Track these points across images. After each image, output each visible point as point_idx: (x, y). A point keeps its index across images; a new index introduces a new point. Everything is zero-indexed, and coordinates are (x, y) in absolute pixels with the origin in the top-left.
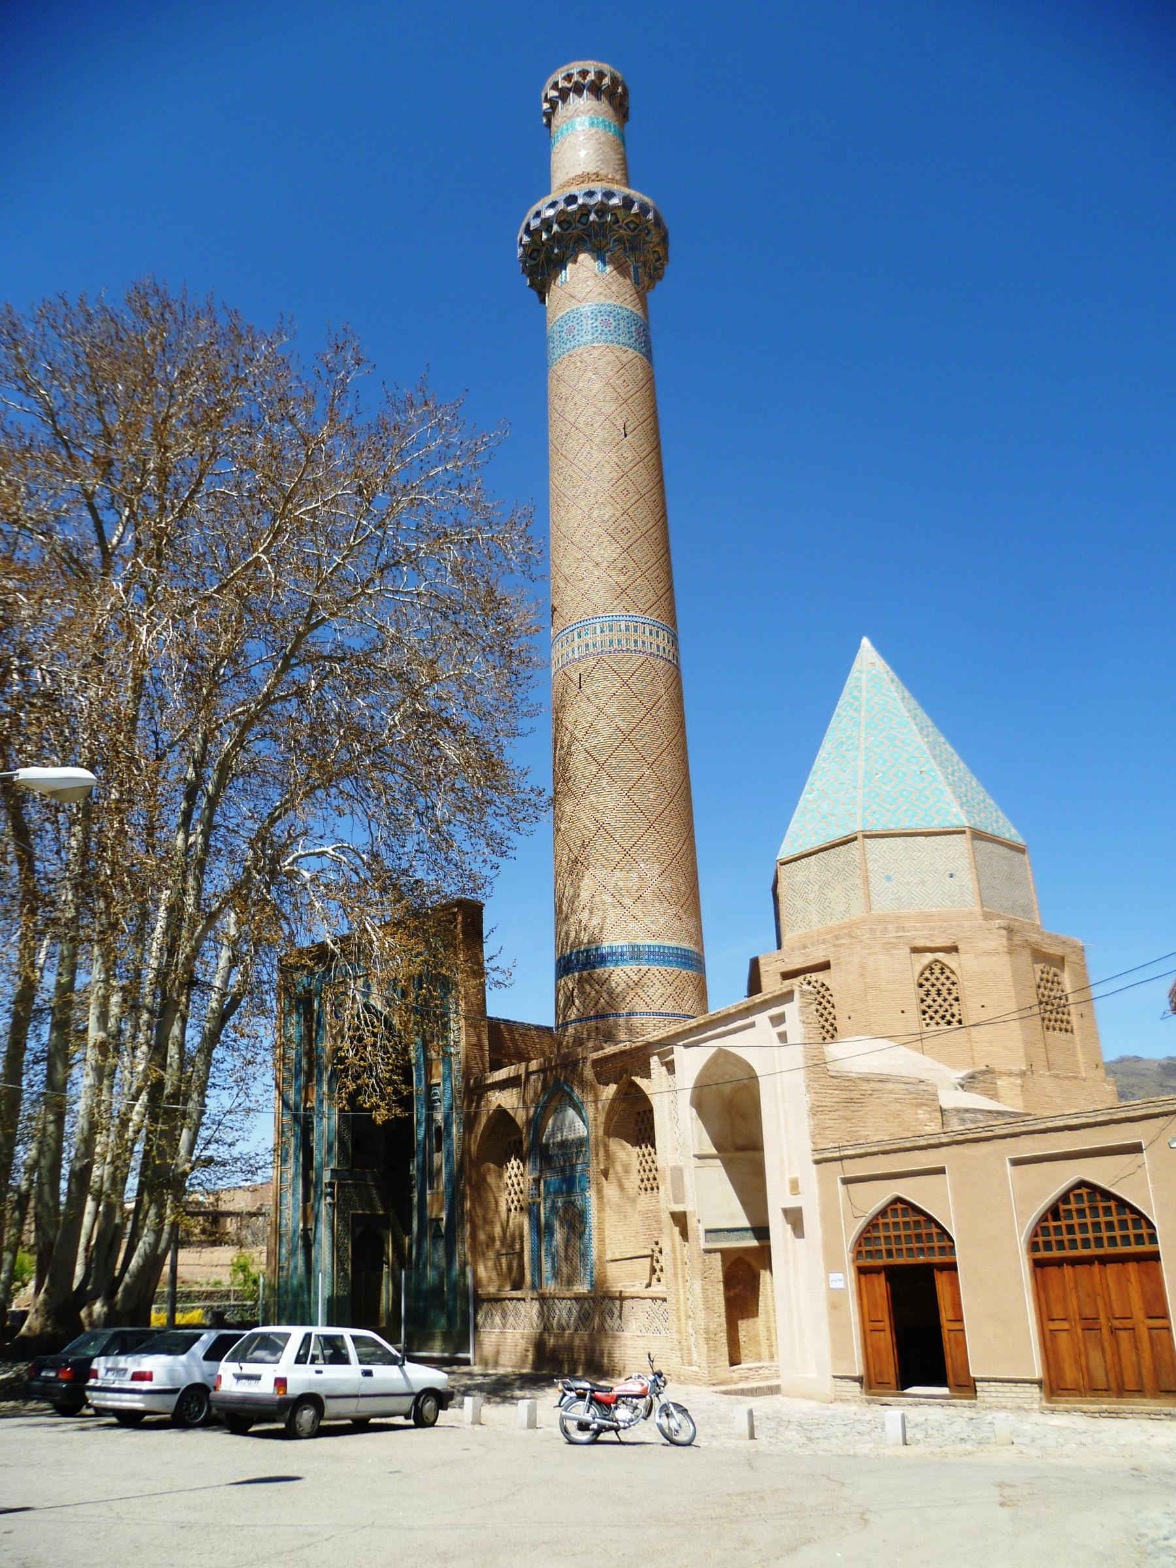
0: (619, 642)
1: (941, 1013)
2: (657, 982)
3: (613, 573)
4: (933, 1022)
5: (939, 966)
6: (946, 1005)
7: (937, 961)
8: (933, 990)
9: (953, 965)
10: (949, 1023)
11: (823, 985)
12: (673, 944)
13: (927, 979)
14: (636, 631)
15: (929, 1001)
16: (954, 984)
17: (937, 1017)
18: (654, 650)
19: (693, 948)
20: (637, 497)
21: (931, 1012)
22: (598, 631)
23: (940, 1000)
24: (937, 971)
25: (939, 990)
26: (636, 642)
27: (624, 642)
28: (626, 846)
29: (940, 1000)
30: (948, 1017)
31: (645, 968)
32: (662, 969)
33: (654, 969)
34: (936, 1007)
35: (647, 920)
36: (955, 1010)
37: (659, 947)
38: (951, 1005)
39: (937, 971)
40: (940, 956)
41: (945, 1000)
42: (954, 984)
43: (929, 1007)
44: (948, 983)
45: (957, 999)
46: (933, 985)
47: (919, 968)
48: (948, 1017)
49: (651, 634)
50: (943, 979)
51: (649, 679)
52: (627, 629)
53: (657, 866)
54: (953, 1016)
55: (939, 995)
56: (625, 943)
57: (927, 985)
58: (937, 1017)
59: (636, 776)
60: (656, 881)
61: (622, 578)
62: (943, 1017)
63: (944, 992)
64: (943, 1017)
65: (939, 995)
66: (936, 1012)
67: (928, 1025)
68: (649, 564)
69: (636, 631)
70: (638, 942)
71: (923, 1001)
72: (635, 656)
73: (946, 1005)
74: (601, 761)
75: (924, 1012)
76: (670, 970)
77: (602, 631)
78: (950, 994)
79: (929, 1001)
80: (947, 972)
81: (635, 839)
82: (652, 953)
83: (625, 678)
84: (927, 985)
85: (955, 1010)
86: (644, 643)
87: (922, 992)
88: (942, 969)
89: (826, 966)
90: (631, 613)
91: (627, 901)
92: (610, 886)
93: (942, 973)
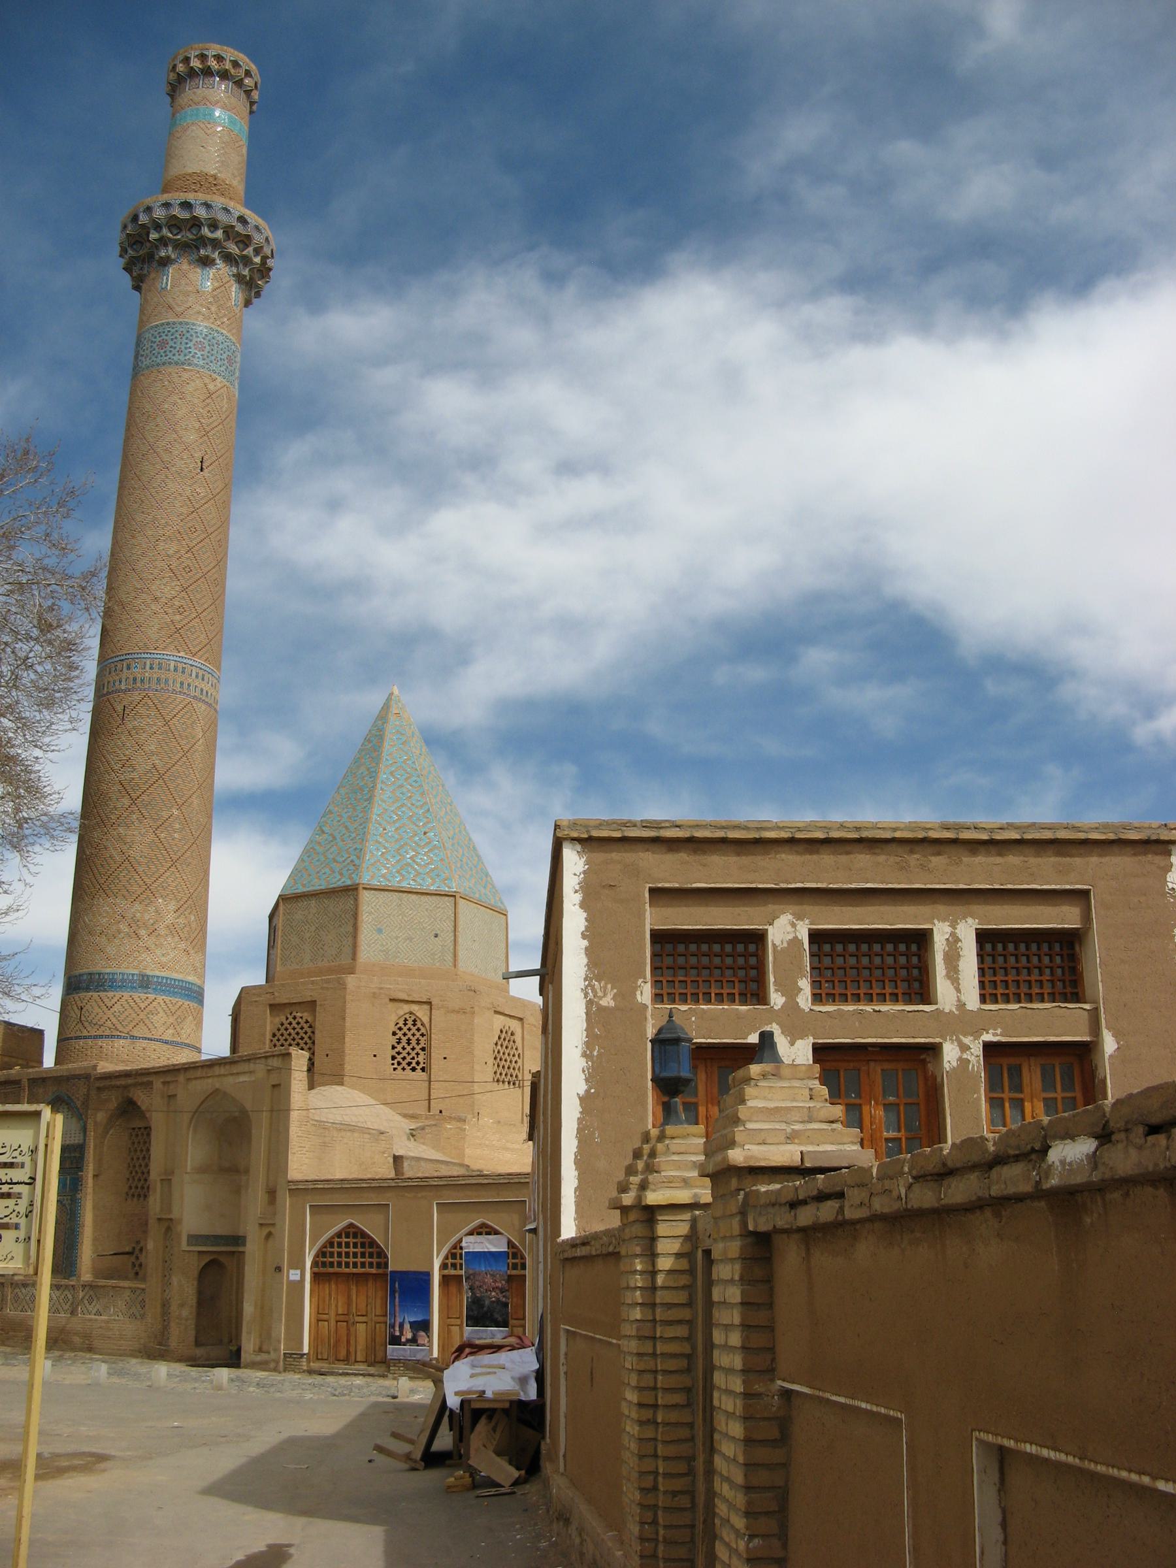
1: (408, 1060)
3: (170, 611)
4: (400, 1068)
6: (413, 1054)
7: (411, 1013)
8: (404, 1039)
9: (426, 1020)
10: (414, 1069)
11: (307, 1022)
13: (400, 1029)
15: (399, 1048)
16: (423, 1035)
17: (404, 1064)
19: (198, 982)
20: (202, 537)
21: (399, 1058)
23: (408, 1048)
24: (410, 1022)
25: (409, 1040)
28: (149, 881)
29: (408, 1048)
30: (414, 1065)
31: (152, 996)
32: (168, 999)
33: (160, 998)
34: (404, 1054)
35: (158, 952)
36: (421, 1059)
38: (418, 1054)
39: (410, 1022)
40: (415, 1008)
41: (413, 1049)
42: (423, 1035)
43: (399, 1053)
44: (418, 1034)
45: (423, 1049)
46: (405, 1035)
47: (394, 1018)
48: (414, 1065)
50: (414, 1029)
53: (173, 902)
54: (418, 1063)
55: (409, 1044)
56: (136, 972)
57: (400, 1034)
58: (404, 1064)
61: (178, 617)
62: (409, 1064)
63: (414, 1042)
64: (409, 1064)
65: (409, 1044)
66: (404, 1058)
67: (395, 1069)
68: (206, 606)
70: (149, 972)
71: (393, 1047)
73: (413, 1054)
75: (393, 1058)
76: (174, 1000)
78: (418, 1044)
79: (399, 1048)
80: (419, 1025)
81: (157, 875)
82: (160, 983)
84: (400, 1034)
85: (421, 1059)
87: (393, 1040)
88: (415, 1021)
89: (311, 1005)
91: (143, 932)
92: (129, 915)
93: (414, 1025)
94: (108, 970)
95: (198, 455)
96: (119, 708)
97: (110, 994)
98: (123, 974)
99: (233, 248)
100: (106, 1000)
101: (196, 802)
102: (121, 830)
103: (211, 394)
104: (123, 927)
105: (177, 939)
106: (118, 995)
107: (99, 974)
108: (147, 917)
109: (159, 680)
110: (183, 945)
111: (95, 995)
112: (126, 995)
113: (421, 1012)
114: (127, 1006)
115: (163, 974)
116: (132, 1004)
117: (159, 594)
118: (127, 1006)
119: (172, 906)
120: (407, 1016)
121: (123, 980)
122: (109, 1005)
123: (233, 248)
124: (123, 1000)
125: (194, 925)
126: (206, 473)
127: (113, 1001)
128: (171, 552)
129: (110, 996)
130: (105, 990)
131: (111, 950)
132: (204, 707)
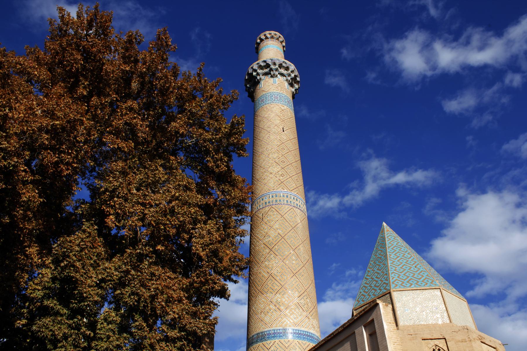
0: (280, 200)
2: (298, 348)
5: (438, 348)
12: (306, 330)
14: (287, 197)
18: (295, 205)
22: (271, 197)
26: (287, 201)
27: (282, 201)
32: (300, 341)
37: (298, 330)
40: (437, 342)
49: (294, 199)
51: (293, 216)
52: (283, 196)
53: (297, 293)
56: (281, 328)
59: (286, 253)
60: (296, 300)
61: (281, 178)
69: (287, 197)
72: (287, 206)
74: (271, 248)
77: (272, 197)
83: (282, 214)
86: (291, 202)
90: (285, 190)
91: (282, 308)
92: (274, 301)
94: (266, 330)
95: (281, 127)
96: (260, 215)
97: (269, 342)
98: (274, 330)
99: (282, 71)
100: (266, 345)
101: (302, 249)
102: (266, 263)
103: (283, 110)
104: (272, 306)
105: (301, 310)
106: (273, 341)
107: (262, 333)
108: (284, 300)
109: (276, 201)
110: (305, 314)
111: (261, 344)
112: (277, 341)
113: (441, 344)
114: (278, 347)
115: (296, 328)
116: (281, 345)
117: (272, 171)
118: (278, 347)
119: (297, 294)
120: (434, 347)
121: (274, 333)
122: (268, 347)
123: (282, 71)
124: (276, 343)
125: (310, 304)
126: (285, 132)
127: (270, 345)
128: (275, 157)
129: (268, 343)
130: (266, 340)
131: (267, 319)
132: (299, 211)
